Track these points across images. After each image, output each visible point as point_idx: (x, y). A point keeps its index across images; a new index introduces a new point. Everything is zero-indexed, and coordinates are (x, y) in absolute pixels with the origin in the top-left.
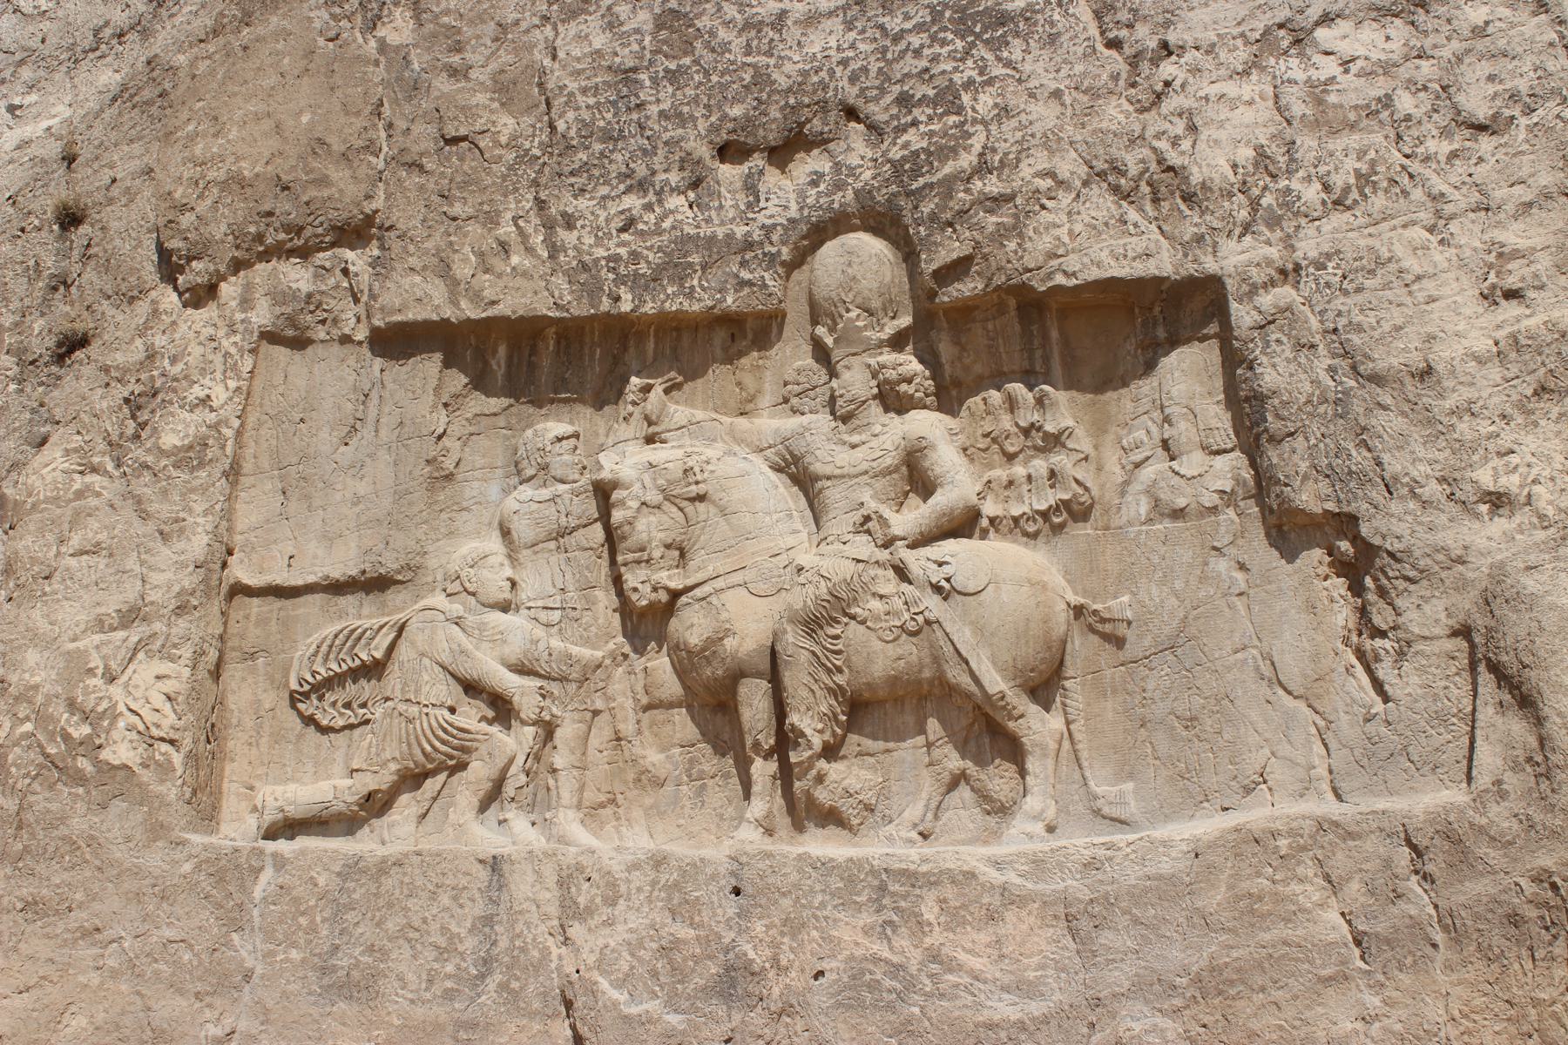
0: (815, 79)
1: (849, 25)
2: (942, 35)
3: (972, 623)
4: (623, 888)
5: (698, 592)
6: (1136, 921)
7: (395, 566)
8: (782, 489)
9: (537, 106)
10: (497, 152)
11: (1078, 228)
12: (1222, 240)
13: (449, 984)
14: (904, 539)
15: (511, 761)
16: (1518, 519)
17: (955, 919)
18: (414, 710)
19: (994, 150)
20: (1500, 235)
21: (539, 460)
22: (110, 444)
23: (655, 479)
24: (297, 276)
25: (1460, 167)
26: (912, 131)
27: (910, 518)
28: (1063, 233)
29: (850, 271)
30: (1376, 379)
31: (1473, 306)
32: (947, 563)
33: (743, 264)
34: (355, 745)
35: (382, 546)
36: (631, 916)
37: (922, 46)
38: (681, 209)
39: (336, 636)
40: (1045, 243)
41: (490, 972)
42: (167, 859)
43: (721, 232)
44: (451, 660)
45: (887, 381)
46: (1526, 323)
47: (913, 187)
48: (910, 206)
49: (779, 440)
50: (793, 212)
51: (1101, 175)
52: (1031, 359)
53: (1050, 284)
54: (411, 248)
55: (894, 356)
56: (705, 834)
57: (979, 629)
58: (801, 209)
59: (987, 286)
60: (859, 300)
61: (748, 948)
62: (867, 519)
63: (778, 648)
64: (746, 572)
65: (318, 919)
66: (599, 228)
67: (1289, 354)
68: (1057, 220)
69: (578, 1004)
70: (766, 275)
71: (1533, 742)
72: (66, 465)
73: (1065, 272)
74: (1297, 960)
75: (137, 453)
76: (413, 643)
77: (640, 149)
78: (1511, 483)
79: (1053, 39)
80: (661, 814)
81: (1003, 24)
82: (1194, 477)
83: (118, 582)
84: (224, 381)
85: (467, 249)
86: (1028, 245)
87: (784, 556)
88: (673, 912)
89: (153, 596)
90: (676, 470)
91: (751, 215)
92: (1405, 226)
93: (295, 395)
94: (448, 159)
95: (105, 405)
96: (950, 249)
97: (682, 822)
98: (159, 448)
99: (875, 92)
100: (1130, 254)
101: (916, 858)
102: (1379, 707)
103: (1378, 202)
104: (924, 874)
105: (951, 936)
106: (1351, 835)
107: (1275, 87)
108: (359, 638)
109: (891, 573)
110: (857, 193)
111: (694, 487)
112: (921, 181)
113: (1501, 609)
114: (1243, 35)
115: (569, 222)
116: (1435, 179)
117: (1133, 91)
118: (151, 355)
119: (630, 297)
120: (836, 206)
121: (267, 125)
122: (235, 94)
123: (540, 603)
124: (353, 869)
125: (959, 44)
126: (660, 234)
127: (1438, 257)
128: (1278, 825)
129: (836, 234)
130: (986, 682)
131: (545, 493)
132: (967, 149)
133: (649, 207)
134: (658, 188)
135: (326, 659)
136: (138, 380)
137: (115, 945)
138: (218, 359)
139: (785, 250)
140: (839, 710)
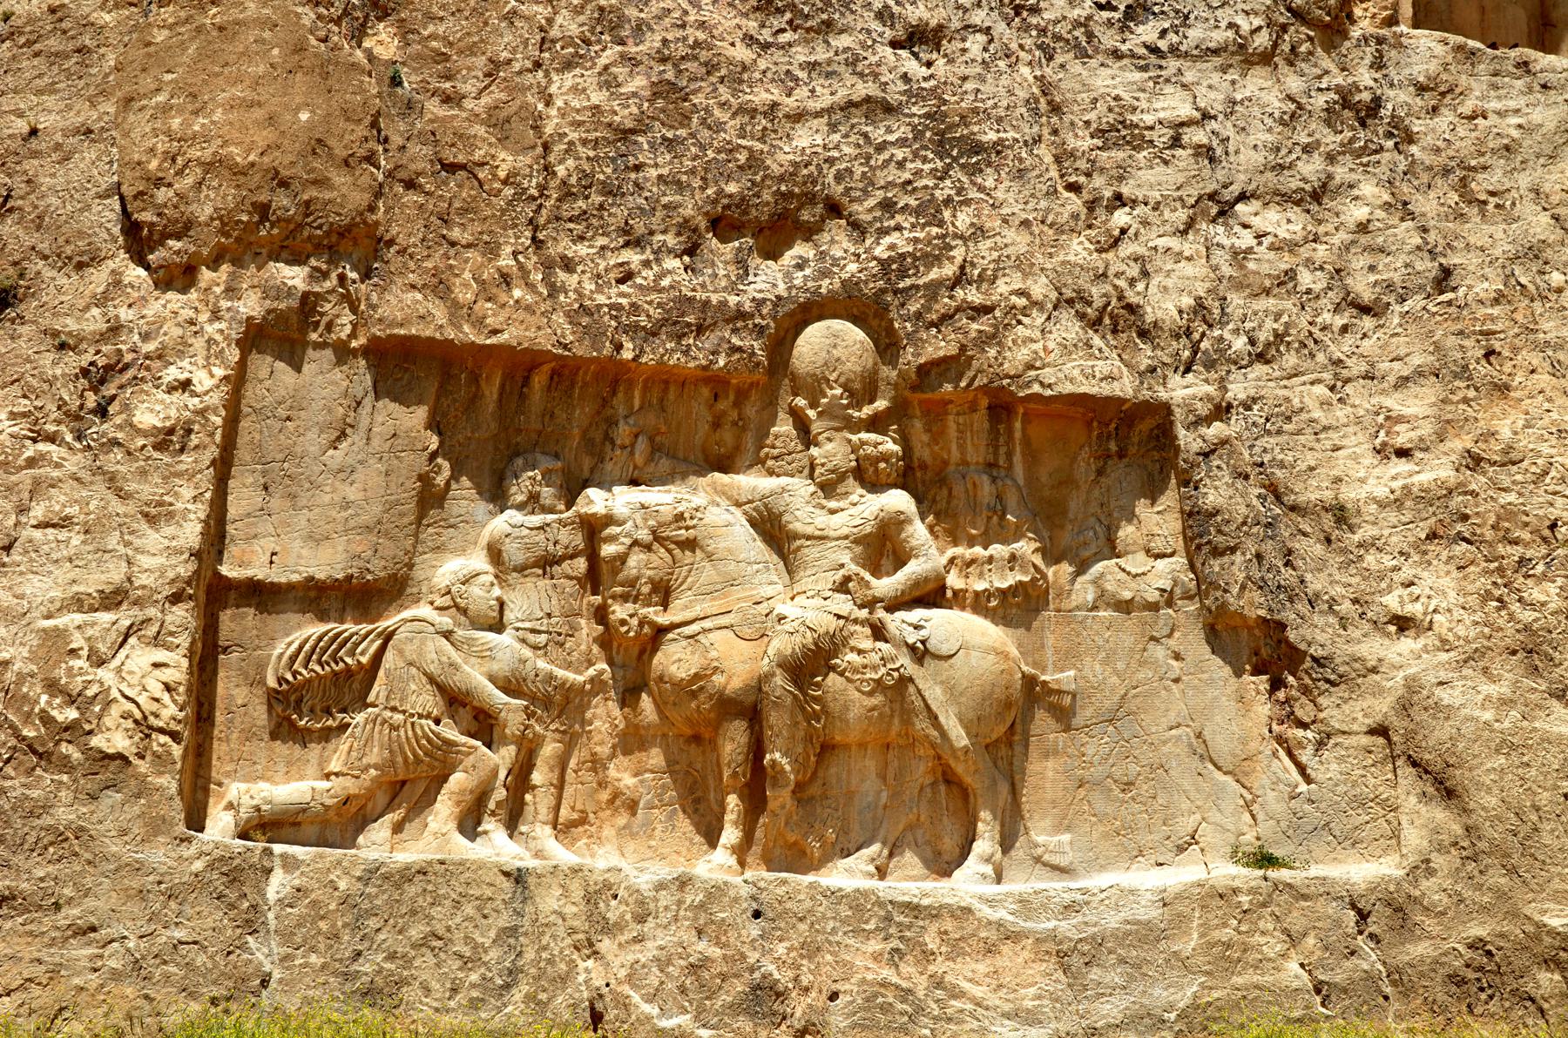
0: (805, 172)
1: (833, 127)
2: (923, 153)
3: (942, 683)
4: (652, 906)
5: (688, 630)
6: (1123, 961)
7: (382, 574)
9: (533, 147)
10: (497, 185)
11: (1051, 345)
12: (1170, 373)
13: (475, 994)
16: (1421, 642)
17: (956, 950)
18: (399, 717)
19: (973, 265)
20: (1388, 402)
22: (67, 414)
23: (646, 520)
24: (294, 276)
25: (1349, 339)
26: (896, 234)
27: (886, 585)
30: (1293, 508)
31: (1370, 459)
32: (922, 627)
33: (735, 331)
35: (369, 553)
36: (659, 933)
37: (905, 159)
39: (320, 639)
40: (1023, 354)
41: (515, 983)
42: (173, 854)
43: (715, 298)
45: (867, 457)
46: (1416, 479)
48: (896, 302)
50: (782, 289)
51: (1070, 302)
52: (996, 453)
53: (1029, 392)
54: (412, 264)
56: (675, 856)
57: (950, 689)
58: (789, 289)
60: (842, 380)
61: (772, 968)
63: (765, 688)
64: (732, 615)
65: (340, 924)
66: (599, 276)
67: (1227, 479)
69: (610, 1015)
71: (1458, 829)
72: (16, 429)
73: (1042, 384)
74: (1269, 1002)
75: (97, 428)
76: (401, 652)
77: (639, 208)
78: (1416, 609)
79: (1021, 174)
80: (633, 836)
81: (977, 153)
82: (1137, 575)
83: (99, 561)
84: (207, 366)
85: (467, 275)
87: (765, 605)
88: (700, 932)
89: (143, 580)
90: (667, 512)
92: (1312, 383)
93: (283, 393)
94: (445, 183)
95: (58, 372)
96: (939, 346)
97: (653, 843)
98: (131, 425)
99: (858, 193)
100: (1098, 375)
101: (917, 892)
102: (1303, 787)
103: (1290, 360)
104: (926, 908)
105: (951, 964)
106: (1305, 897)
107: (1208, 249)
109: (868, 631)
110: (843, 282)
111: (683, 532)
112: (908, 282)
113: (1419, 715)
114: (1181, 199)
115: (568, 265)
116: (1333, 348)
117: (1093, 233)
118: (115, 329)
120: (823, 291)
121: (258, 113)
122: (217, 75)
123: (527, 625)
124: (372, 873)
125: (939, 164)
126: (660, 291)
127: (1339, 413)
128: (1237, 883)
129: (820, 318)
130: (953, 738)
132: (951, 259)
133: (646, 264)
134: (655, 247)
135: (308, 660)
136: (98, 352)
137: (115, 945)
138: (199, 344)
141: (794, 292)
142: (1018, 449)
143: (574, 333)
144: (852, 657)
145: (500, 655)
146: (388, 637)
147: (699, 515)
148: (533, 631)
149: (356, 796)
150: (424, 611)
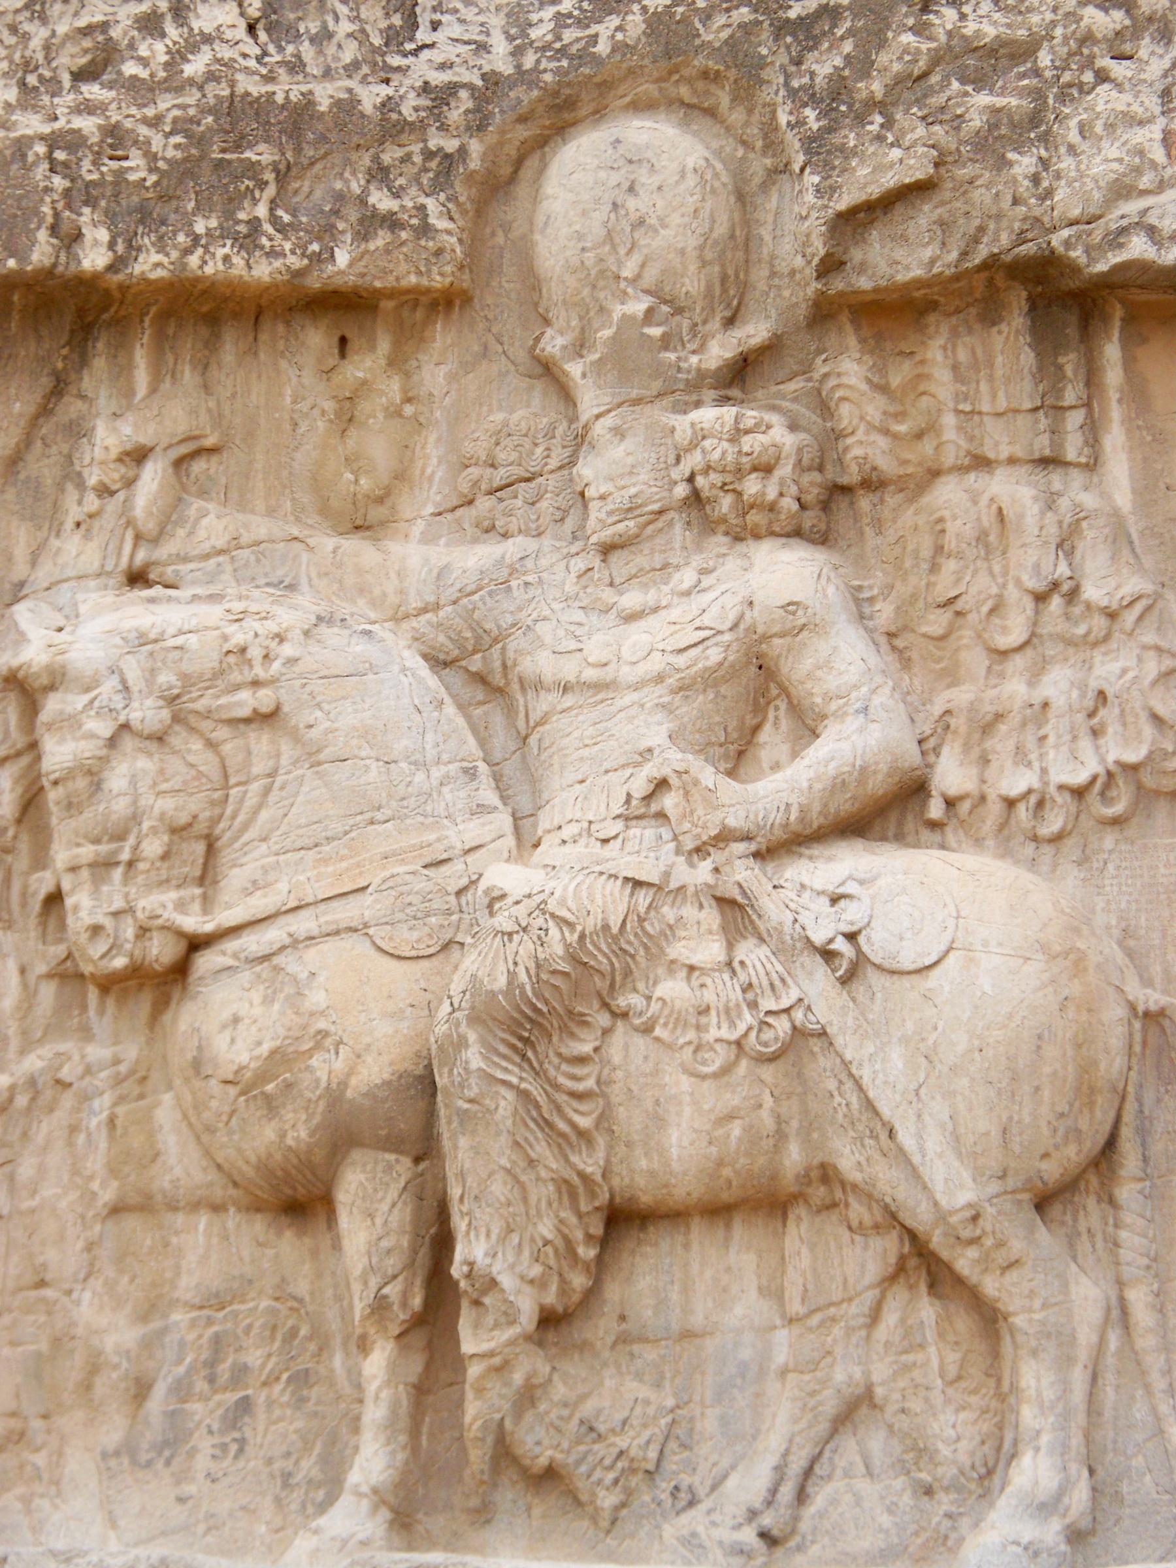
3: (905, 1040)
5: (251, 942)
8: (450, 709)
14: (748, 838)
23: (153, 672)
29: (632, 203)
33: (380, 174)
38: (229, 34)
43: (325, 95)
47: (792, 14)
48: (782, 58)
49: (451, 593)
50: (500, 59)
53: (1116, 258)
55: (729, 413)
58: (517, 52)
59: (964, 254)
60: (650, 277)
62: (662, 784)
64: (367, 899)
66: (28, 66)
68: (1136, 108)
70: (431, 203)
86: (1066, 163)
87: (458, 866)
91: (395, 61)
97: (190, 1489)
109: (711, 917)
111: (244, 695)
119: (103, 235)
126: (179, 90)
133: (150, 24)
139: (475, 147)
140: (579, 1235)
141: (529, 61)
142: (1116, 413)
144: (673, 989)
147: (288, 650)
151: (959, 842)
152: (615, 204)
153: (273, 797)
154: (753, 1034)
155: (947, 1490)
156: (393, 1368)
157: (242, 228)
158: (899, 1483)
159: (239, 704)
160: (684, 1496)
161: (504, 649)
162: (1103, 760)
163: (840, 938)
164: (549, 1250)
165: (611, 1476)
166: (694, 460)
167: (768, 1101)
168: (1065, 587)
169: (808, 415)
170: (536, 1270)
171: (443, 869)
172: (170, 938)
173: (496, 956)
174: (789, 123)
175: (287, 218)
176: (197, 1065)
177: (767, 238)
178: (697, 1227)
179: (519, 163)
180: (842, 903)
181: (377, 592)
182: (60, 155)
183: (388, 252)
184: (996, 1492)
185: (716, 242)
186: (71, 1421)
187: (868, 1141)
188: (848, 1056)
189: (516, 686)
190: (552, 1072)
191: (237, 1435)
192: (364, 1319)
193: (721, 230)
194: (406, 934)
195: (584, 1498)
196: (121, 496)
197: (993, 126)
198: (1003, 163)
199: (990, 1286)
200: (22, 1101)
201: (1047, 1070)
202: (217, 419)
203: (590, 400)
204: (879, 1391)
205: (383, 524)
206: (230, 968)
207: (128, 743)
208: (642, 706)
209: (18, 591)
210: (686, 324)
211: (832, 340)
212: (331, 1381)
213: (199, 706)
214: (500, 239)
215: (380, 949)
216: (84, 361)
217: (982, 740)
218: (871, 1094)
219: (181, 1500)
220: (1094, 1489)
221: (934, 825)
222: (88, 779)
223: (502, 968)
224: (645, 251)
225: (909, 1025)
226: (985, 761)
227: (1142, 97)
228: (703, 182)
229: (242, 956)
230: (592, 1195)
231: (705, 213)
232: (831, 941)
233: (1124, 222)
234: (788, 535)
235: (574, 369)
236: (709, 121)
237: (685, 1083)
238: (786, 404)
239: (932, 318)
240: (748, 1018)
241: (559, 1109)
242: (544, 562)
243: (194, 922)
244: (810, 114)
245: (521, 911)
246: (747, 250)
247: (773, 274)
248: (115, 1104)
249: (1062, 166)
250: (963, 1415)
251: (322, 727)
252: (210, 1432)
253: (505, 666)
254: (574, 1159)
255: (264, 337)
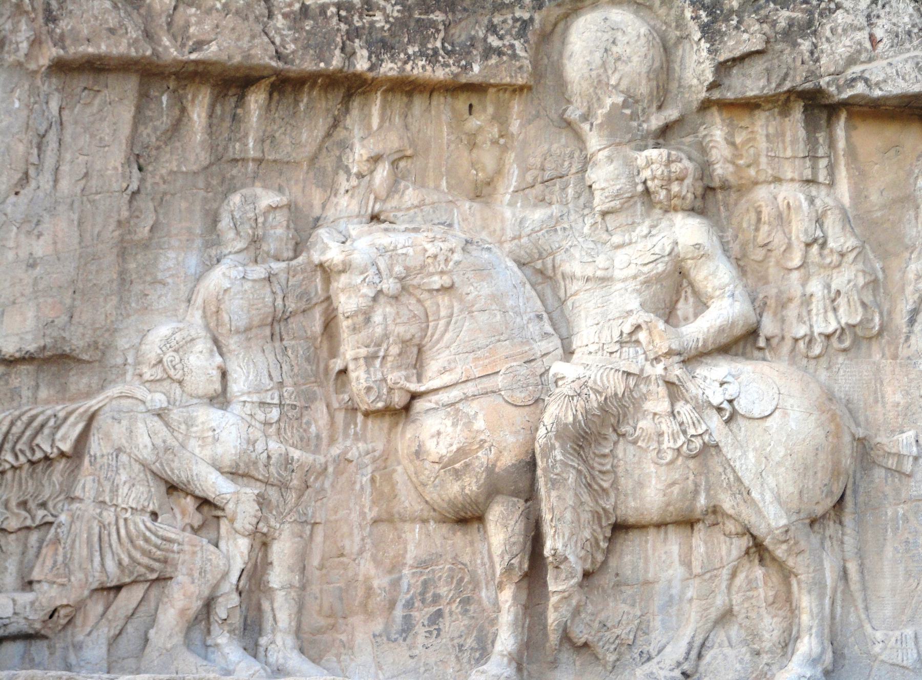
3: (755, 449)
5: (445, 397)
7: (81, 343)
8: (528, 286)
11: (879, 33)
14: (679, 354)
15: (225, 575)
21: (250, 232)
28: (863, 36)
29: (615, 49)
33: (492, 29)
34: (31, 552)
35: (65, 318)
39: (12, 424)
40: (842, 48)
44: (154, 458)
49: (528, 230)
52: (814, 168)
55: (664, 152)
59: (779, 85)
62: (638, 327)
64: (499, 378)
68: (855, 22)
70: (517, 43)
73: (866, 81)
76: (107, 436)
86: (825, 46)
97: (416, 652)
108: (42, 426)
109: (662, 390)
111: (436, 278)
119: (365, 53)
123: (255, 398)
131: (259, 272)
140: (601, 537)
142: (842, 161)
143: (295, 40)
145: (224, 436)
146: (92, 418)
147: (456, 257)
148: (262, 404)
149: (63, 606)
150: (129, 386)
151: (772, 357)
152: (606, 50)
153: (451, 327)
154: (685, 446)
155: (767, 653)
156: (515, 598)
157: (430, 52)
158: (744, 650)
159: (435, 282)
160: (645, 656)
161: (553, 260)
162: (839, 323)
163: (726, 402)
164: (588, 543)
165: (613, 647)
166: (646, 174)
167: (692, 477)
168: (820, 241)
169: (695, 154)
170: (583, 553)
171: (533, 364)
172: (404, 394)
173: (567, 407)
174: (692, 17)
175: (449, 48)
176: (417, 454)
177: (677, 68)
178: (652, 531)
179: (555, 25)
180: (725, 386)
181: (492, 229)
182: (343, 13)
183: (497, 66)
184: (790, 653)
185: (655, 70)
186: (357, 620)
187: (737, 496)
188: (729, 456)
189: (559, 277)
190: (591, 462)
191: (437, 627)
192: (502, 574)
193: (657, 64)
194: (519, 395)
195: (601, 657)
196: (367, 178)
197: (791, 25)
198: (795, 45)
199: (791, 563)
200: (331, 469)
201: (820, 465)
202: (412, 143)
203: (594, 141)
204: (736, 608)
205: (490, 195)
206: (433, 409)
207: (382, 299)
208: (626, 290)
209: (317, 223)
210: (640, 108)
211: (708, 118)
212: (480, 602)
213: (415, 282)
214: (546, 61)
215: (507, 402)
216: (347, 111)
217: (782, 311)
218: (740, 474)
219: (411, 657)
220: (834, 652)
221: (760, 349)
222: (364, 316)
223: (570, 413)
224: (621, 73)
225: (757, 443)
226: (783, 321)
227: (859, 17)
228: (648, 41)
229: (440, 403)
230: (608, 519)
231: (650, 57)
232: (722, 403)
233: (854, 76)
234: (689, 210)
235: (586, 127)
236: (648, 12)
237: (652, 468)
238: (685, 148)
239: (757, 112)
240: (682, 439)
241: (594, 478)
242: (572, 218)
243: (414, 387)
244: (703, 14)
245: (576, 386)
246: (668, 74)
247: (680, 86)
248: (373, 471)
249: (824, 47)
250: (775, 620)
251: (473, 295)
252: (424, 625)
253: (554, 266)
254: (601, 502)
255: (434, 103)
